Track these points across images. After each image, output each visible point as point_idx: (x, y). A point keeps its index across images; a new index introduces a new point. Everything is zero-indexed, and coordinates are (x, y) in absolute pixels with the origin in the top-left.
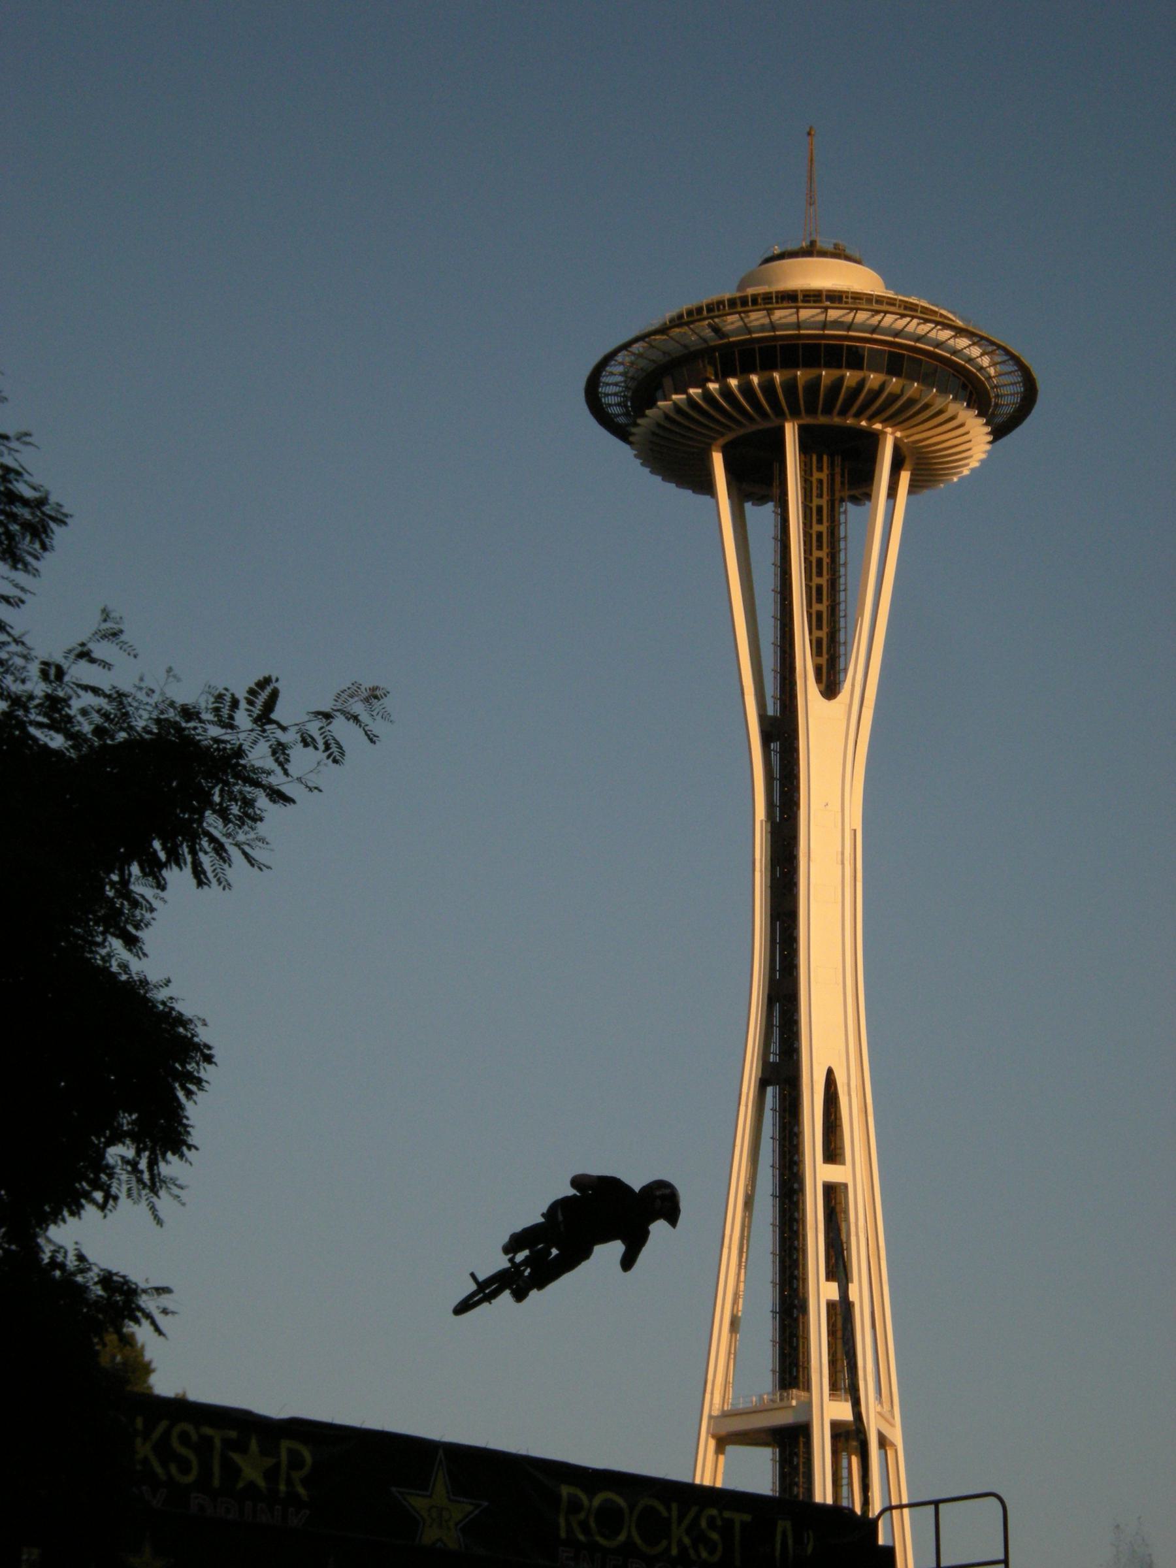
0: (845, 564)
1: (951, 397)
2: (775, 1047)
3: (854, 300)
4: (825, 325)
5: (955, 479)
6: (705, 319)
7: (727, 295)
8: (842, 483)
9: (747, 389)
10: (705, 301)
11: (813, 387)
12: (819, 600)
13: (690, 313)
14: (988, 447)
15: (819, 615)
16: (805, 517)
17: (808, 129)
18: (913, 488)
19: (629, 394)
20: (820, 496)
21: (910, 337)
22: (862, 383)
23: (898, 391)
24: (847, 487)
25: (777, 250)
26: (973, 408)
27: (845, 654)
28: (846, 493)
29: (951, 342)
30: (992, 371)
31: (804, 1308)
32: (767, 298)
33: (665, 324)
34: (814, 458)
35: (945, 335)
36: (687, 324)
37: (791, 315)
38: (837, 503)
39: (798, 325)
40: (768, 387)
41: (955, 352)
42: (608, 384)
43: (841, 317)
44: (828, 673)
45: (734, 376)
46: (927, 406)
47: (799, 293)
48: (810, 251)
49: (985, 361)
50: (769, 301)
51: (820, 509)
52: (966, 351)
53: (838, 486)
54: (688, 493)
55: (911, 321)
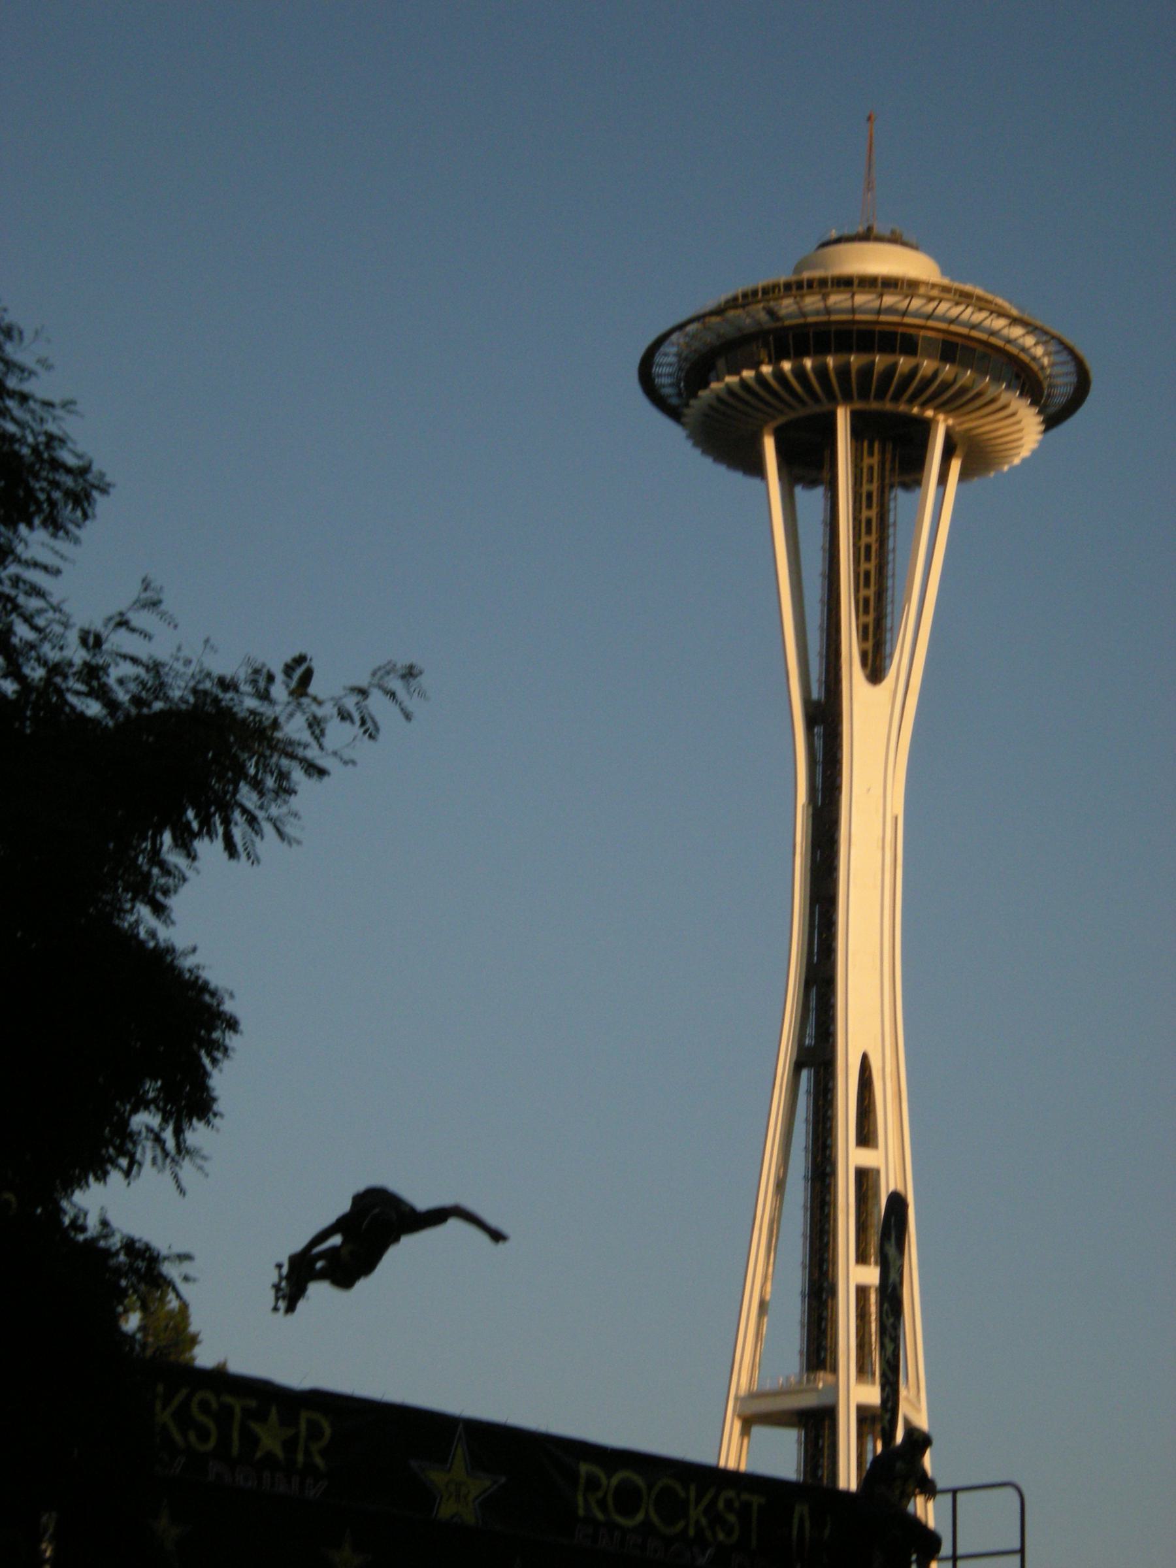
0: (894, 550)
1: (1004, 386)
2: (811, 1030)
3: (909, 286)
4: (879, 311)
5: (1006, 468)
6: (759, 302)
7: (783, 279)
8: (893, 469)
9: (799, 372)
10: (761, 283)
11: (866, 372)
12: (867, 584)
13: (745, 295)
14: (1039, 437)
15: (866, 601)
16: (855, 502)
17: (867, 114)
18: (964, 476)
19: (683, 374)
20: (871, 481)
21: (965, 324)
22: (915, 370)
23: (951, 377)
24: (897, 472)
25: (834, 234)
26: (1026, 395)
27: (892, 640)
28: (897, 479)
29: (1005, 332)
30: (1046, 361)
31: (833, 1292)
32: (823, 282)
33: (720, 305)
34: (866, 444)
35: (999, 323)
36: (743, 306)
37: (846, 300)
38: (887, 490)
39: (853, 311)
40: (822, 371)
41: (1009, 341)
42: (661, 365)
43: (896, 303)
44: (874, 661)
45: (786, 357)
46: (979, 395)
47: (855, 279)
48: (867, 236)
49: (1039, 351)
50: (824, 285)
51: (869, 496)
52: (1021, 341)
53: (887, 473)
54: (737, 479)
55: (964, 310)
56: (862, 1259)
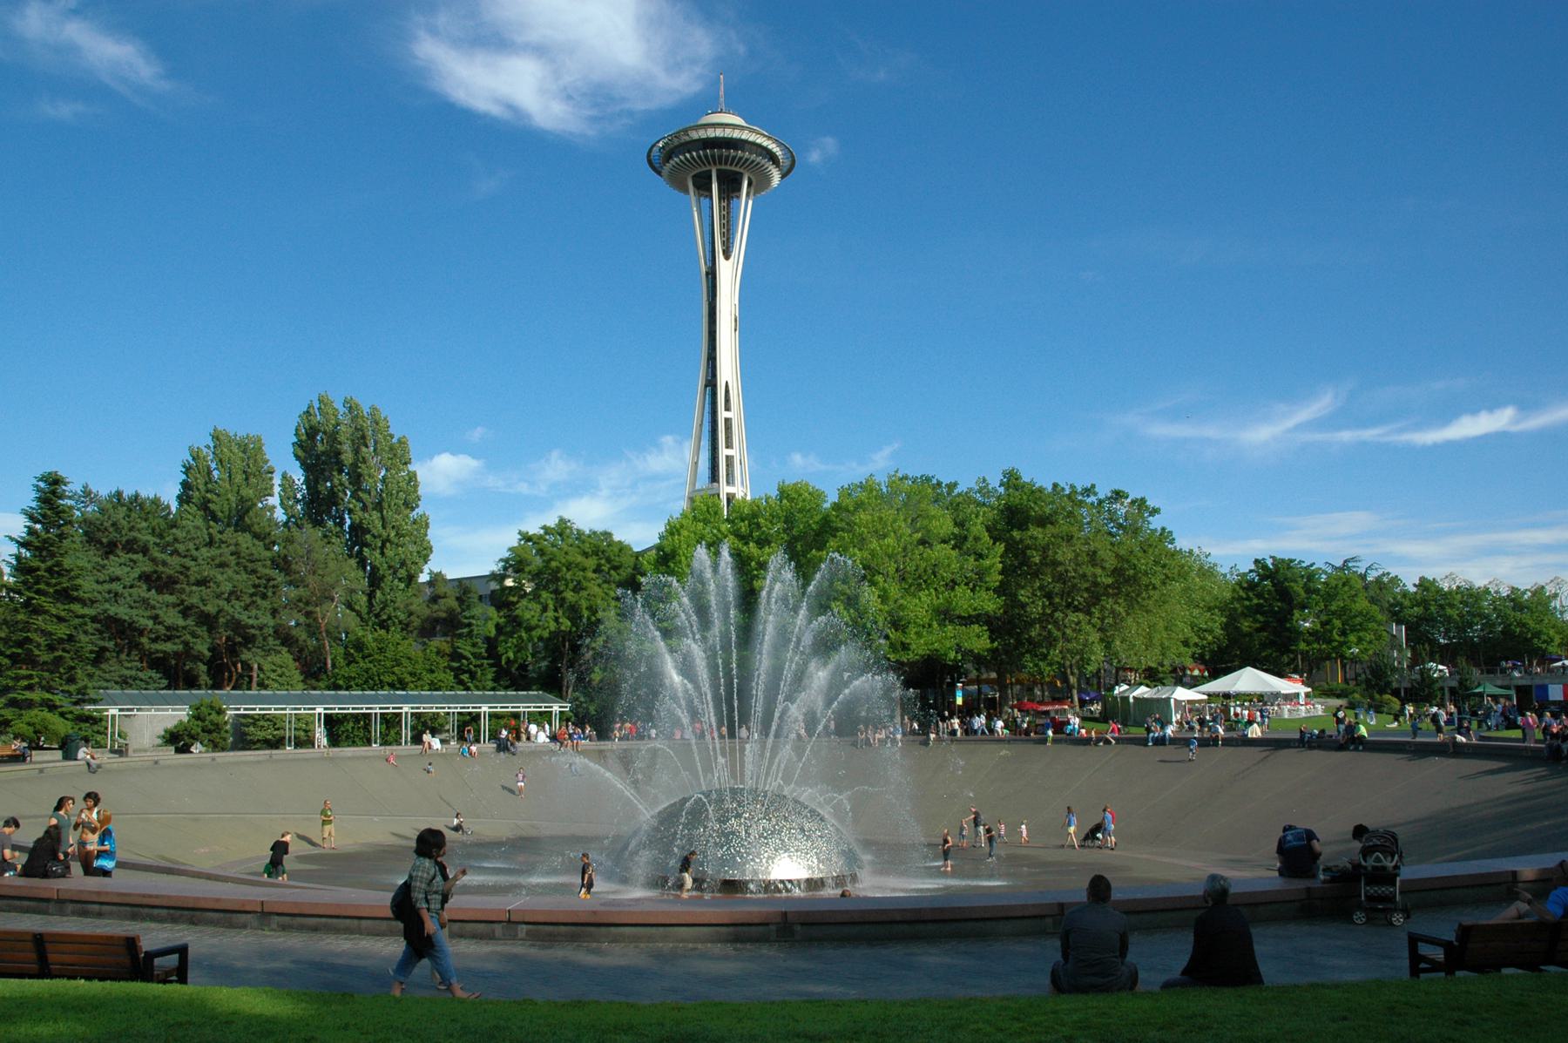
3: (734, 126)
56: (727, 447)
